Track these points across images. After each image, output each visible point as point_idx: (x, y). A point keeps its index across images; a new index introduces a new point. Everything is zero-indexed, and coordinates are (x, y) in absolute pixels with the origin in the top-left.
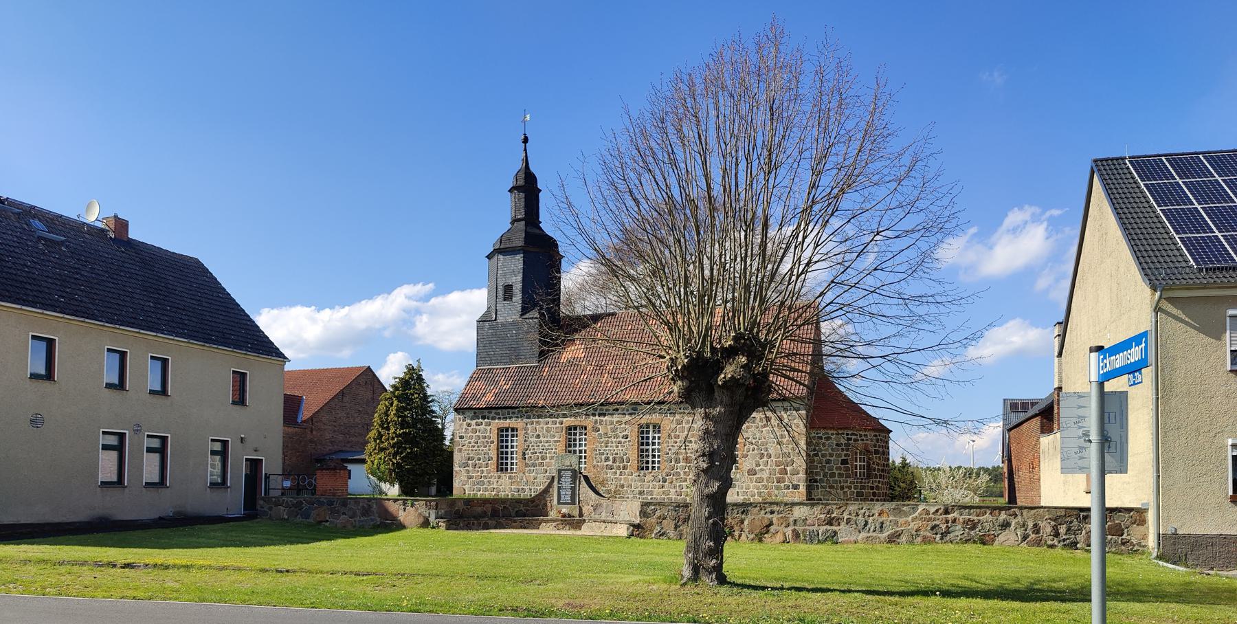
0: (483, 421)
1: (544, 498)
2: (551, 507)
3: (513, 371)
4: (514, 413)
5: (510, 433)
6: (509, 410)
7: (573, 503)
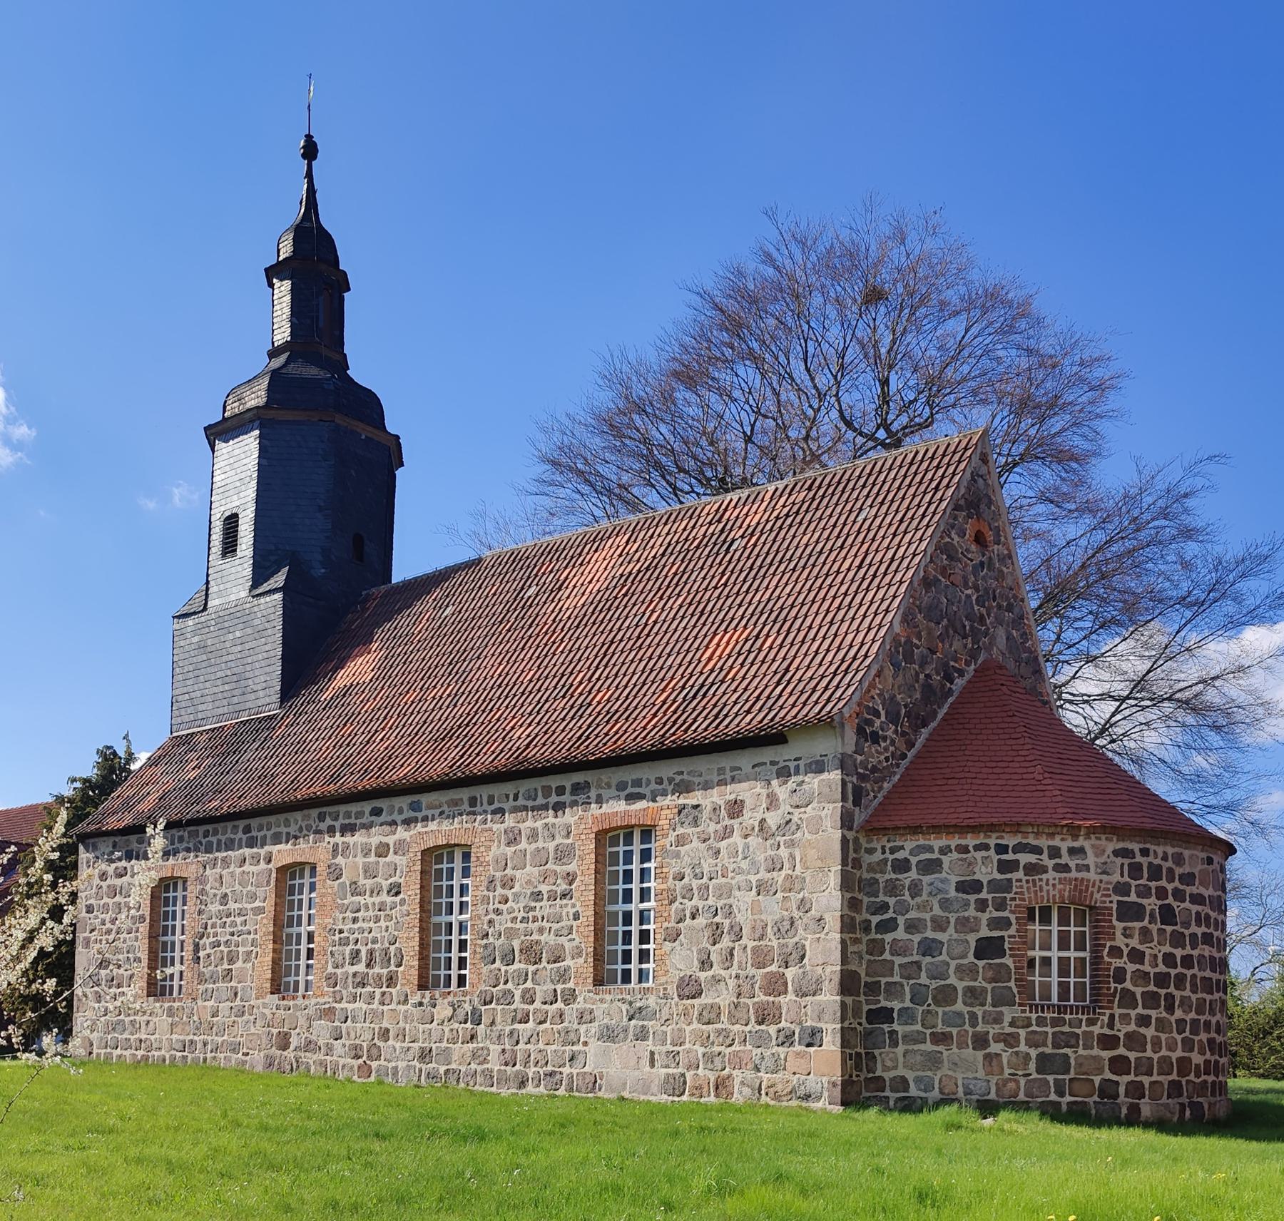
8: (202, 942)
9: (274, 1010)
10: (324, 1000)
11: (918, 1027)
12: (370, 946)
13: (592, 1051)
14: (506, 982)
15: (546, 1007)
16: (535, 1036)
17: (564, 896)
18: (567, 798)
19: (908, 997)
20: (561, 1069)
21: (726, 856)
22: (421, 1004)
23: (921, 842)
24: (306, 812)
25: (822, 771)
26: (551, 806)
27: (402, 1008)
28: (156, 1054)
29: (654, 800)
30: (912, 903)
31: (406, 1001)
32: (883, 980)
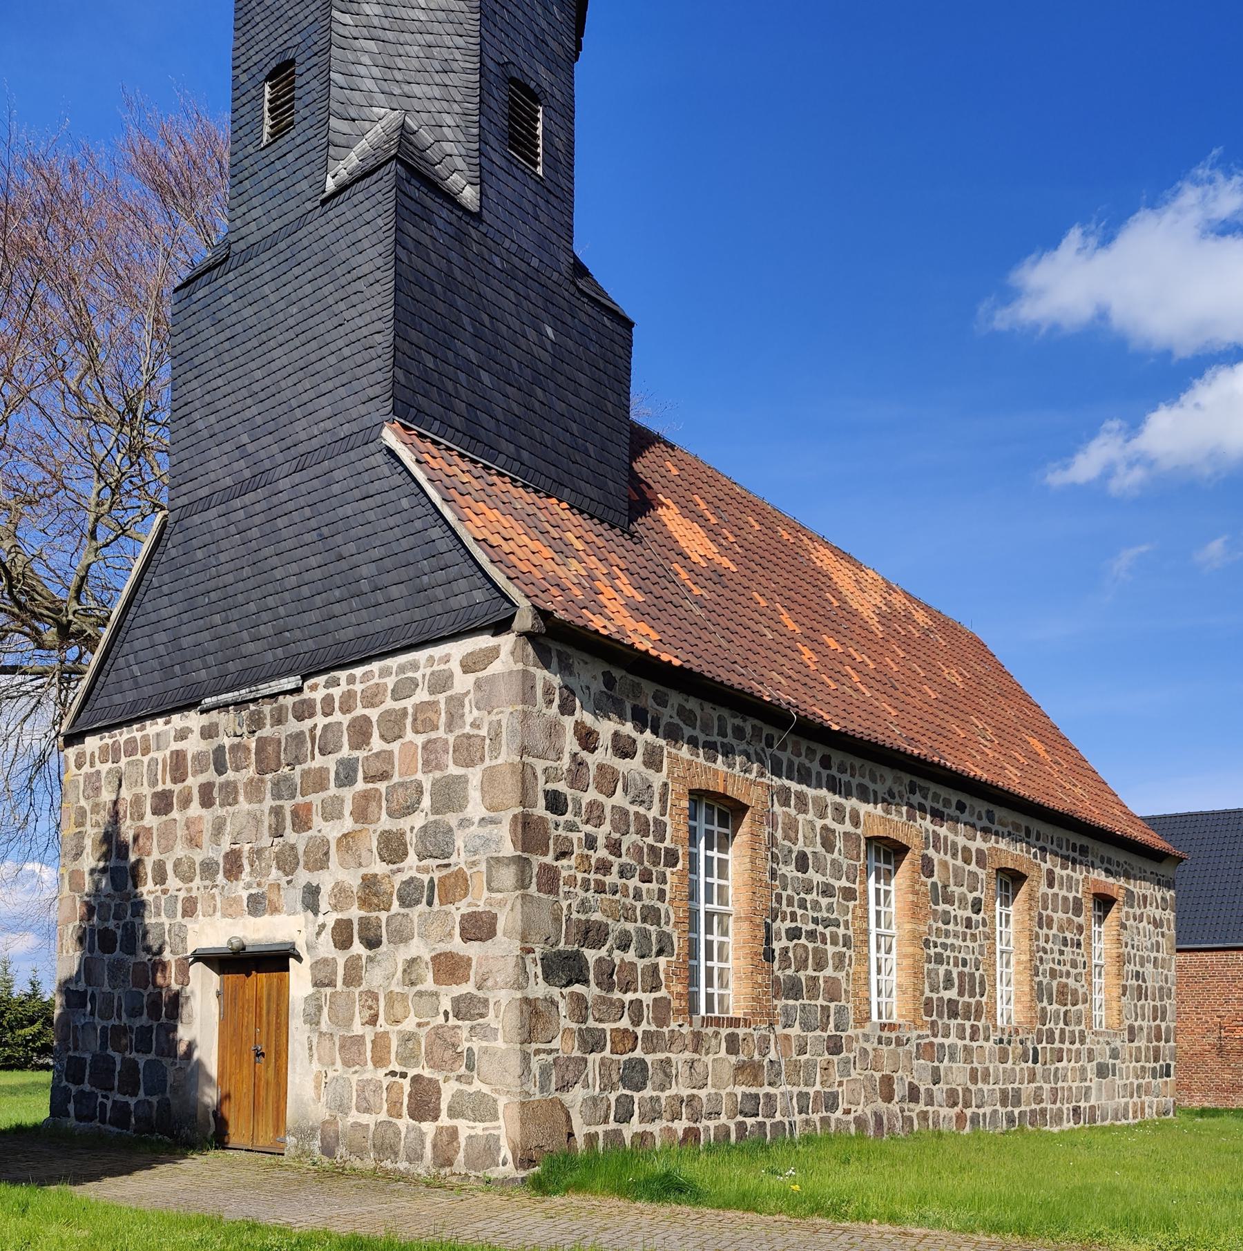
8: (775, 926)
28: (712, 1124)
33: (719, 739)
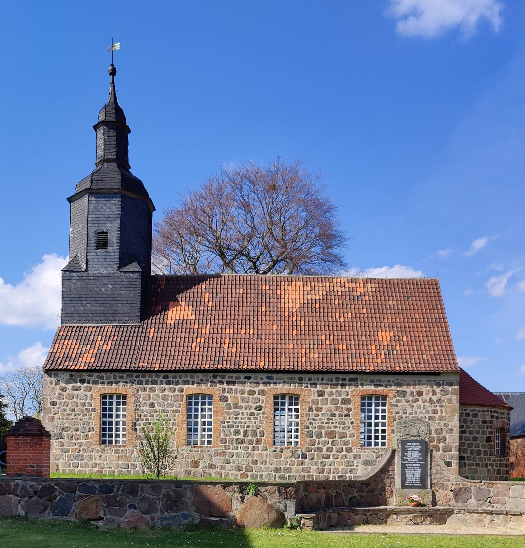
0: (82, 386)
1: (382, 480)
2: (392, 492)
3: (110, 330)
4: (121, 377)
5: (114, 400)
6: (116, 374)
7: (423, 486)
8: (137, 423)
9: (189, 452)
10: (219, 449)
11: (472, 462)
12: (245, 429)
13: (360, 468)
14: (318, 445)
15: (338, 453)
16: (333, 463)
17: (346, 415)
18: (347, 382)
19: (469, 453)
20: (345, 475)
21: (416, 408)
22: (275, 451)
23: (473, 408)
24: (206, 374)
25: (452, 385)
26: (339, 384)
27: (265, 453)
28: (108, 470)
29: (386, 387)
30: (470, 426)
31: (266, 450)
32: (462, 448)
33: (114, 380)
